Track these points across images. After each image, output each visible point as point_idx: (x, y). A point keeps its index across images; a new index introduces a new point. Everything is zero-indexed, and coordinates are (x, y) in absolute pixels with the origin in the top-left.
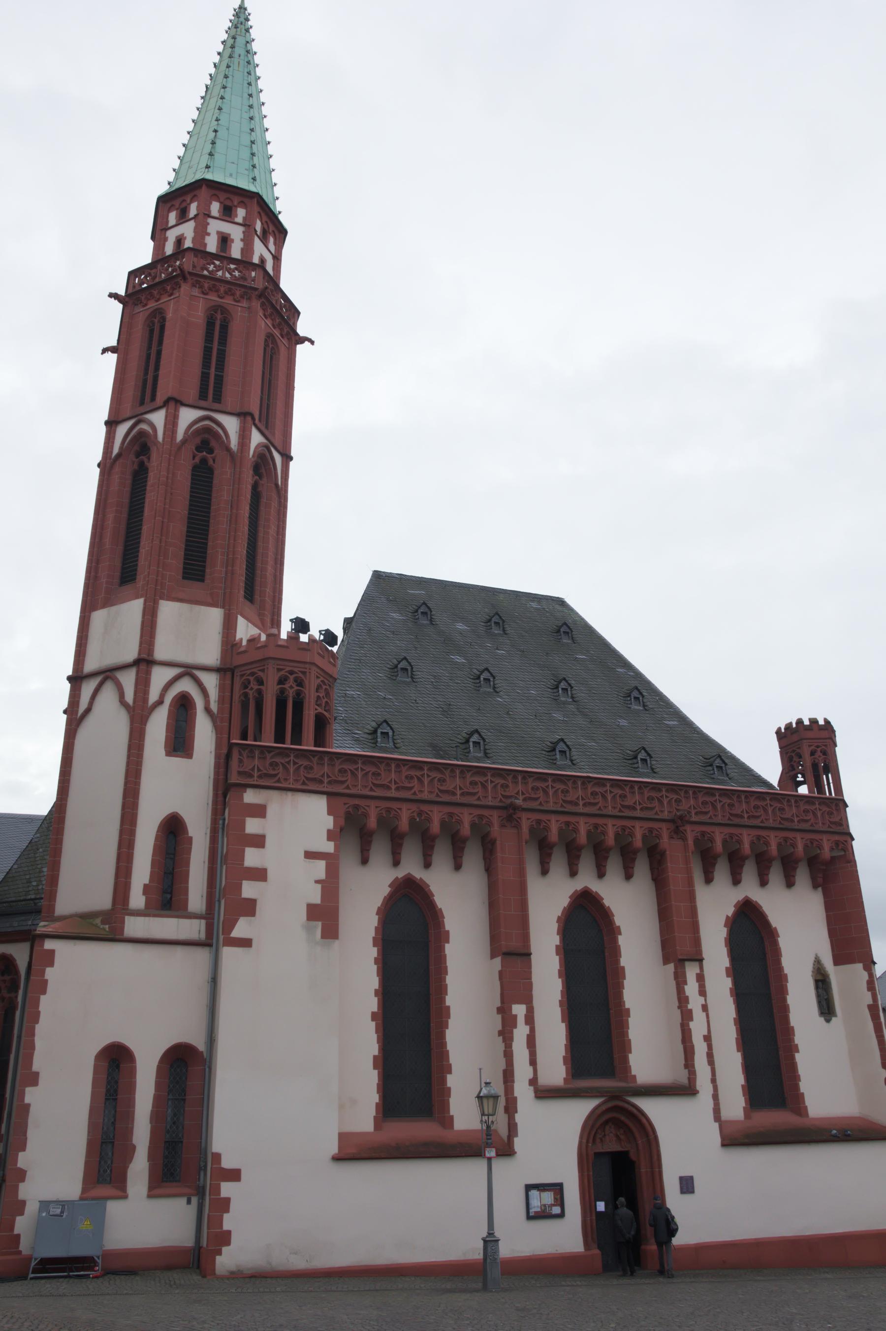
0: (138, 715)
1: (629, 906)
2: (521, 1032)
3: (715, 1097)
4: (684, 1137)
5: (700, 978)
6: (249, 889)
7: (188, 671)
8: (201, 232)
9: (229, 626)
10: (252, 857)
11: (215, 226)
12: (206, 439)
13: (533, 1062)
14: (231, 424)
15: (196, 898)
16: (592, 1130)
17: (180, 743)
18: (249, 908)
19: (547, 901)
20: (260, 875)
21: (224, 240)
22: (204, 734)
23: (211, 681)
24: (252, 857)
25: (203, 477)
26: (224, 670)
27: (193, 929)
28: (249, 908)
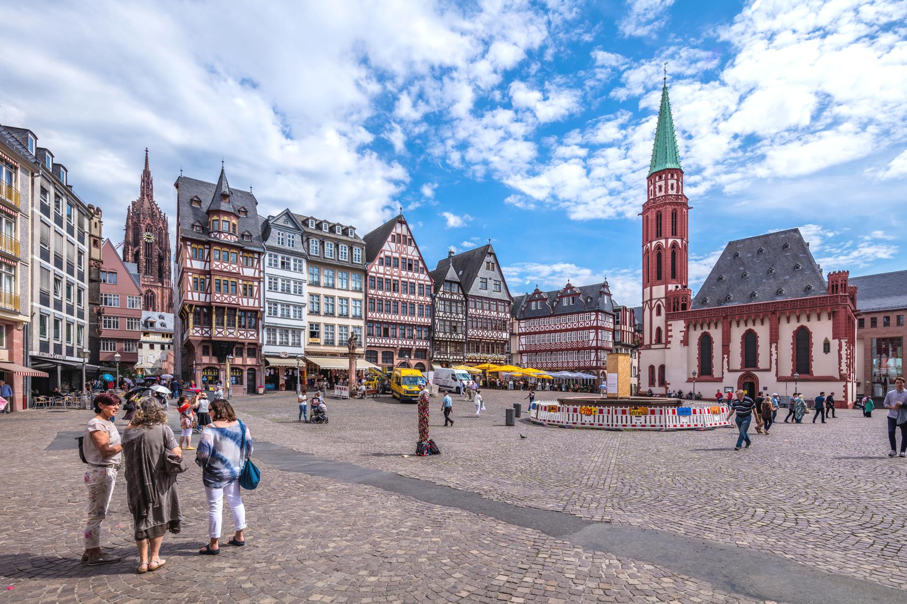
0: (651, 309)
1: (762, 331)
2: (726, 360)
3: (777, 372)
4: (767, 381)
5: (776, 347)
6: (669, 339)
7: (659, 299)
8: (655, 188)
9: (666, 288)
10: (670, 334)
11: (658, 184)
12: (659, 247)
13: (728, 365)
14: (663, 241)
15: (664, 341)
16: (741, 378)
17: (659, 314)
18: (670, 342)
19: (737, 333)
20: (671, 336)
21: (660, 187)
22: (663, 310)
23: (663, 300)
24: (670, 334)
25: (659, 256)
26: (666, 298)
27: (663, 346)
28: (670, 342)
